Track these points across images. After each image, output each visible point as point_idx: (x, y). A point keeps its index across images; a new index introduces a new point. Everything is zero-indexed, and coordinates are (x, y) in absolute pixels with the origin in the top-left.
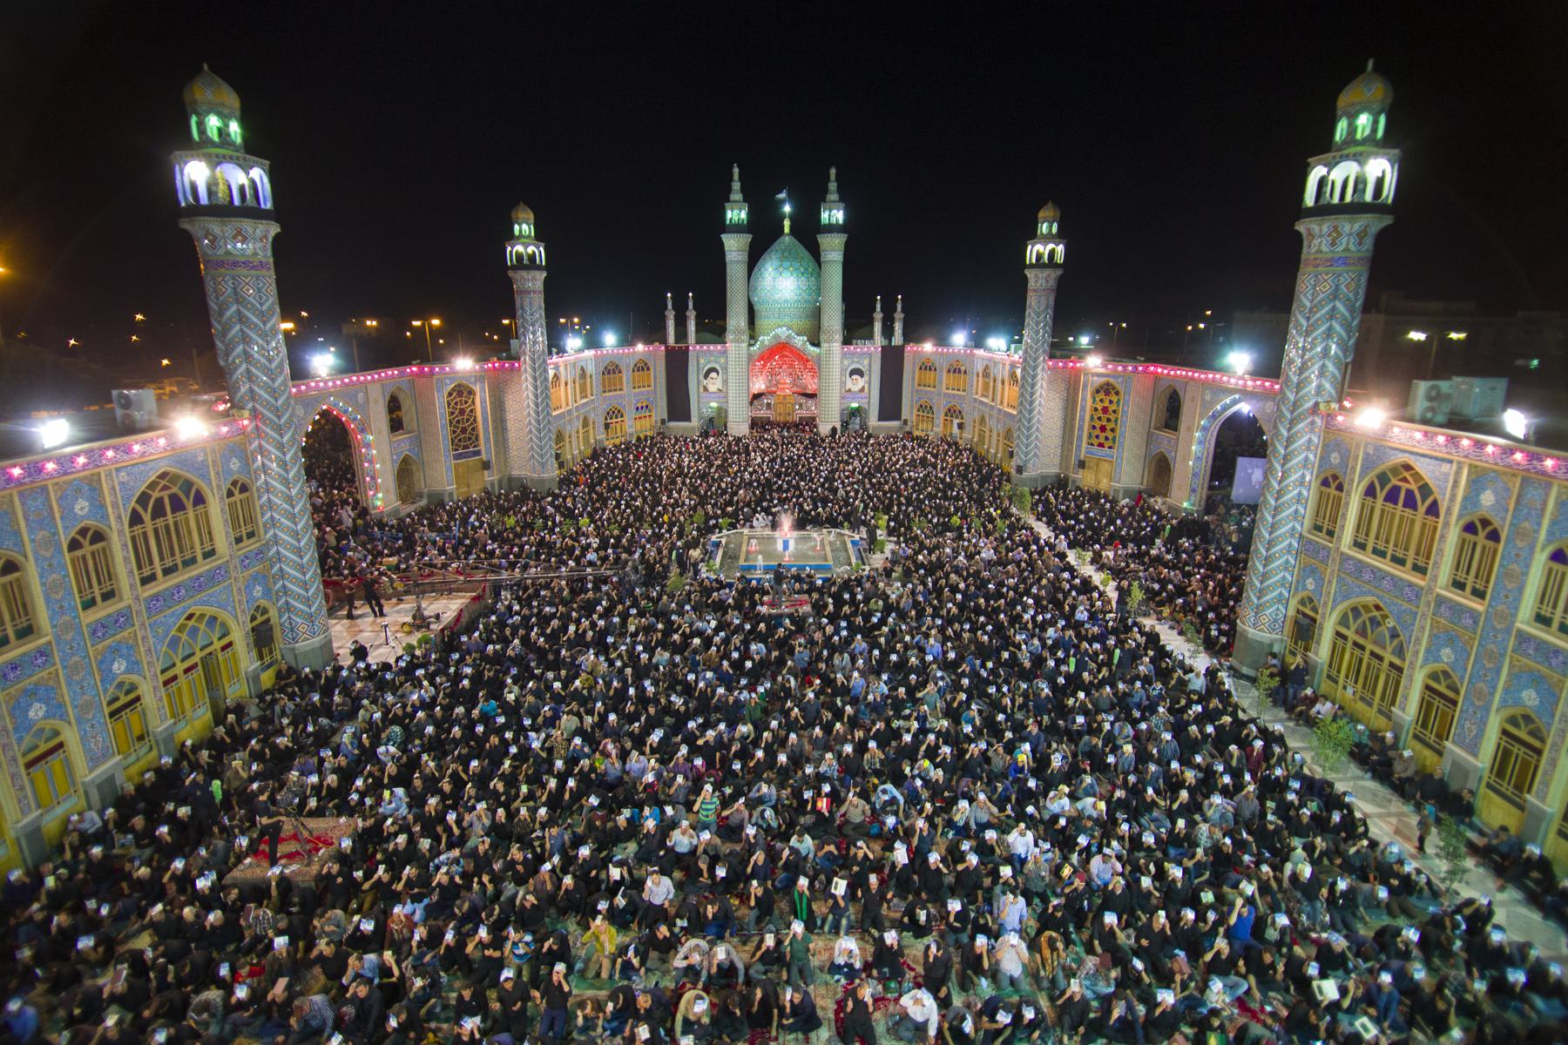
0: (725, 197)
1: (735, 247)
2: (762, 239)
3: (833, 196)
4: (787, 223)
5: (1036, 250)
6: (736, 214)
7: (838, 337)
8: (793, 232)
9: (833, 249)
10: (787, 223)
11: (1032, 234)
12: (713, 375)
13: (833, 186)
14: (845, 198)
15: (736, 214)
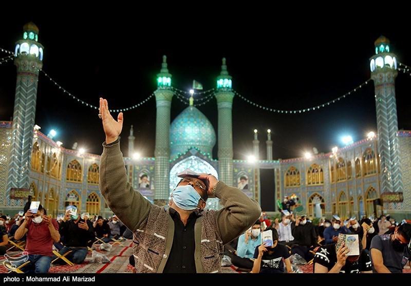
0: (157, 69)
1: (162, 101)
2: (177, 108)
3: (225, 72)
4: (191, 100)
5: (376, 63)
6: (164, 80)
7: (231, 154)
8: (195, 103)
9: (225, 104)
10: (191, 100)
11: (371, 54)
12: (145, 178)
13: (224, 67)
14: (233, 74)
15: (164, 80)
